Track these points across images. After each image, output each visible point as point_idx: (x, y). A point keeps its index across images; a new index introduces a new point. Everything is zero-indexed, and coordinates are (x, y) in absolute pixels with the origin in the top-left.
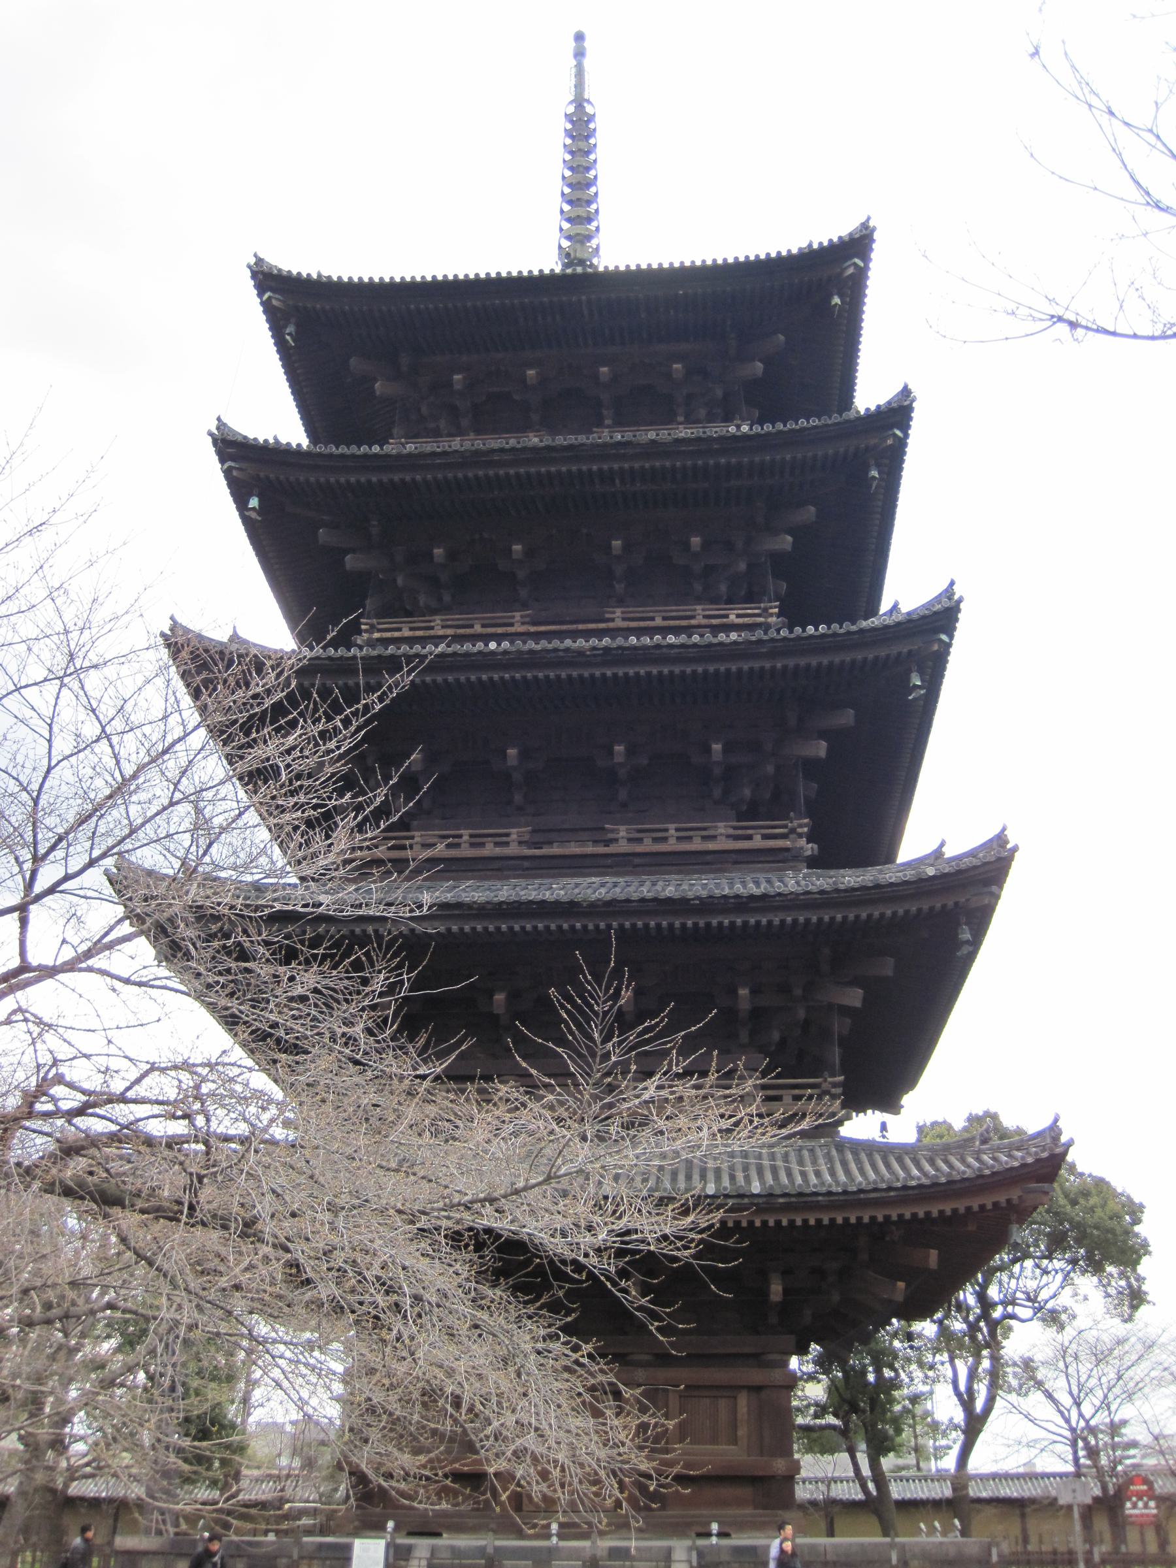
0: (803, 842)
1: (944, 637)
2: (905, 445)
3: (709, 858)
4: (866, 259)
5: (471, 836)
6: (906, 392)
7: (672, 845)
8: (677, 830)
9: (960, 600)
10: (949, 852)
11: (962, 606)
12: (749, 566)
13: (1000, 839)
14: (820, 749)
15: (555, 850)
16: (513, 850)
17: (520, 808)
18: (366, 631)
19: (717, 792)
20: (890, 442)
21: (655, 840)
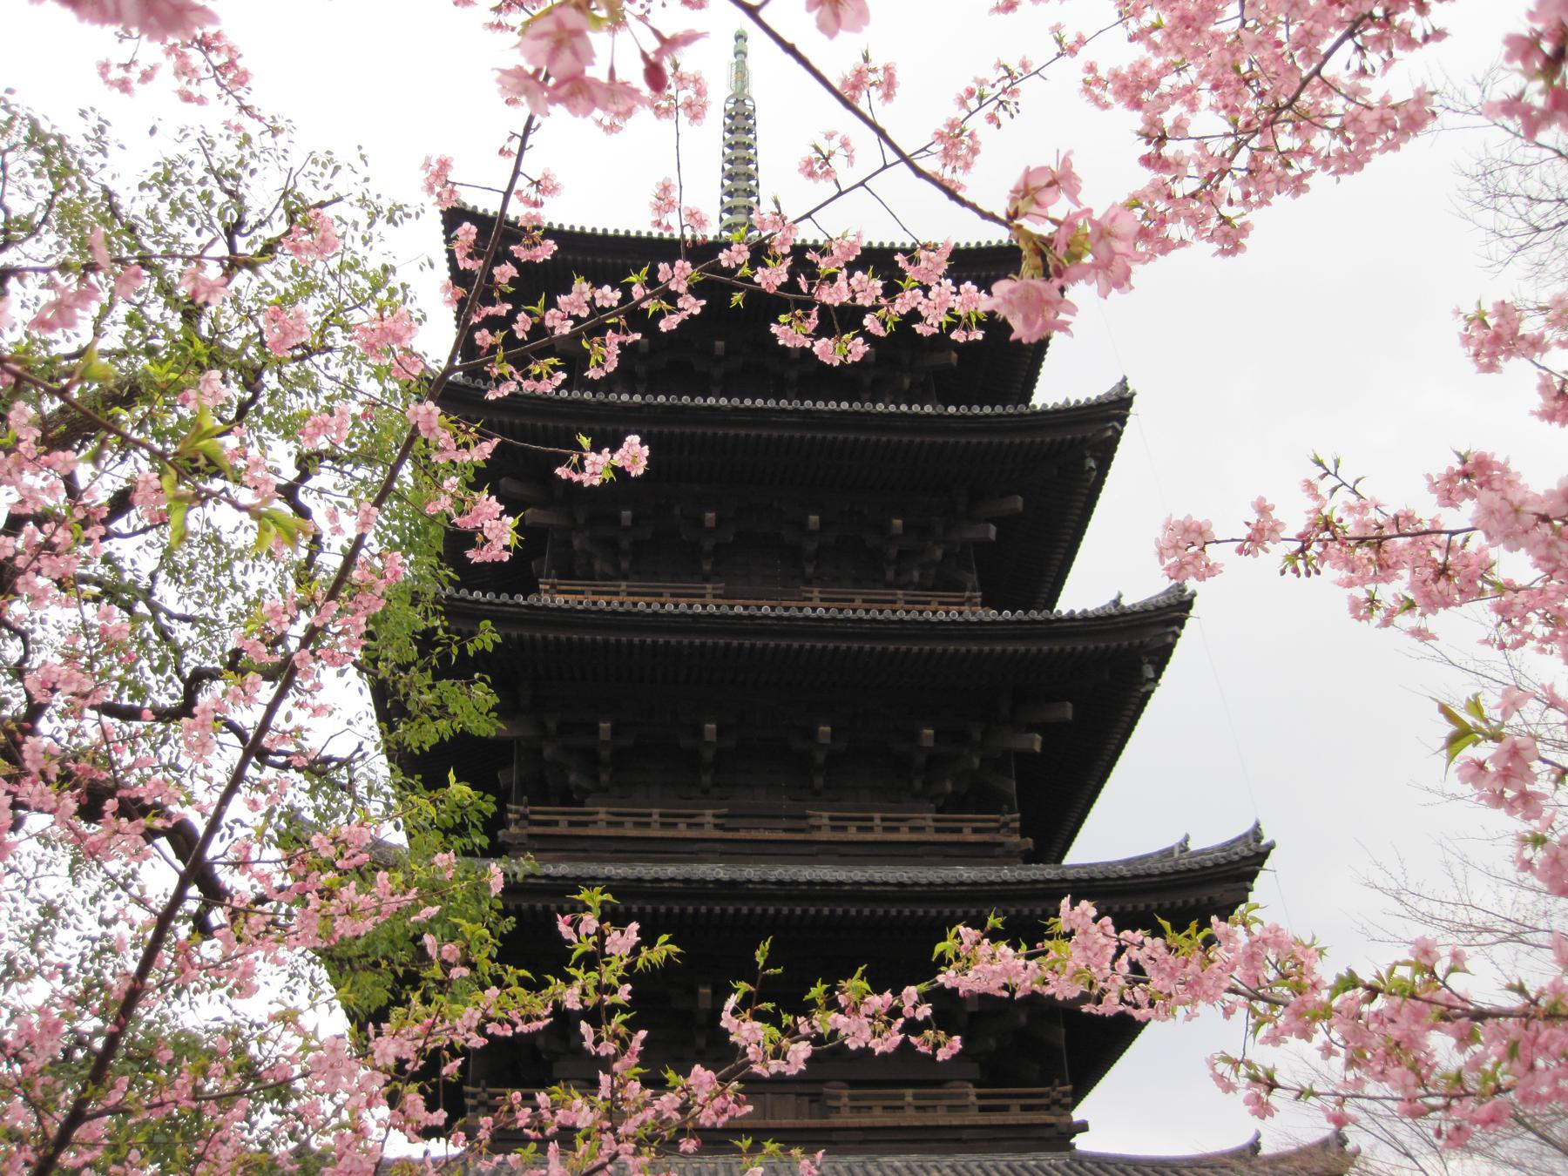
0: (1016, 839)
1: (1176, 628)
2: (1117, 441)
3: (921, 850)
5: (662, 815)
8: (883, 819)
10: (1194, 846)
11: (1196, 600)
12: (945, 555)
13: (1256, 833)
15: (742, 835)
17: (706, 791)
18: (546, 591)
19: (918, 784)
20: (1110, 433)
21: (860, 829)
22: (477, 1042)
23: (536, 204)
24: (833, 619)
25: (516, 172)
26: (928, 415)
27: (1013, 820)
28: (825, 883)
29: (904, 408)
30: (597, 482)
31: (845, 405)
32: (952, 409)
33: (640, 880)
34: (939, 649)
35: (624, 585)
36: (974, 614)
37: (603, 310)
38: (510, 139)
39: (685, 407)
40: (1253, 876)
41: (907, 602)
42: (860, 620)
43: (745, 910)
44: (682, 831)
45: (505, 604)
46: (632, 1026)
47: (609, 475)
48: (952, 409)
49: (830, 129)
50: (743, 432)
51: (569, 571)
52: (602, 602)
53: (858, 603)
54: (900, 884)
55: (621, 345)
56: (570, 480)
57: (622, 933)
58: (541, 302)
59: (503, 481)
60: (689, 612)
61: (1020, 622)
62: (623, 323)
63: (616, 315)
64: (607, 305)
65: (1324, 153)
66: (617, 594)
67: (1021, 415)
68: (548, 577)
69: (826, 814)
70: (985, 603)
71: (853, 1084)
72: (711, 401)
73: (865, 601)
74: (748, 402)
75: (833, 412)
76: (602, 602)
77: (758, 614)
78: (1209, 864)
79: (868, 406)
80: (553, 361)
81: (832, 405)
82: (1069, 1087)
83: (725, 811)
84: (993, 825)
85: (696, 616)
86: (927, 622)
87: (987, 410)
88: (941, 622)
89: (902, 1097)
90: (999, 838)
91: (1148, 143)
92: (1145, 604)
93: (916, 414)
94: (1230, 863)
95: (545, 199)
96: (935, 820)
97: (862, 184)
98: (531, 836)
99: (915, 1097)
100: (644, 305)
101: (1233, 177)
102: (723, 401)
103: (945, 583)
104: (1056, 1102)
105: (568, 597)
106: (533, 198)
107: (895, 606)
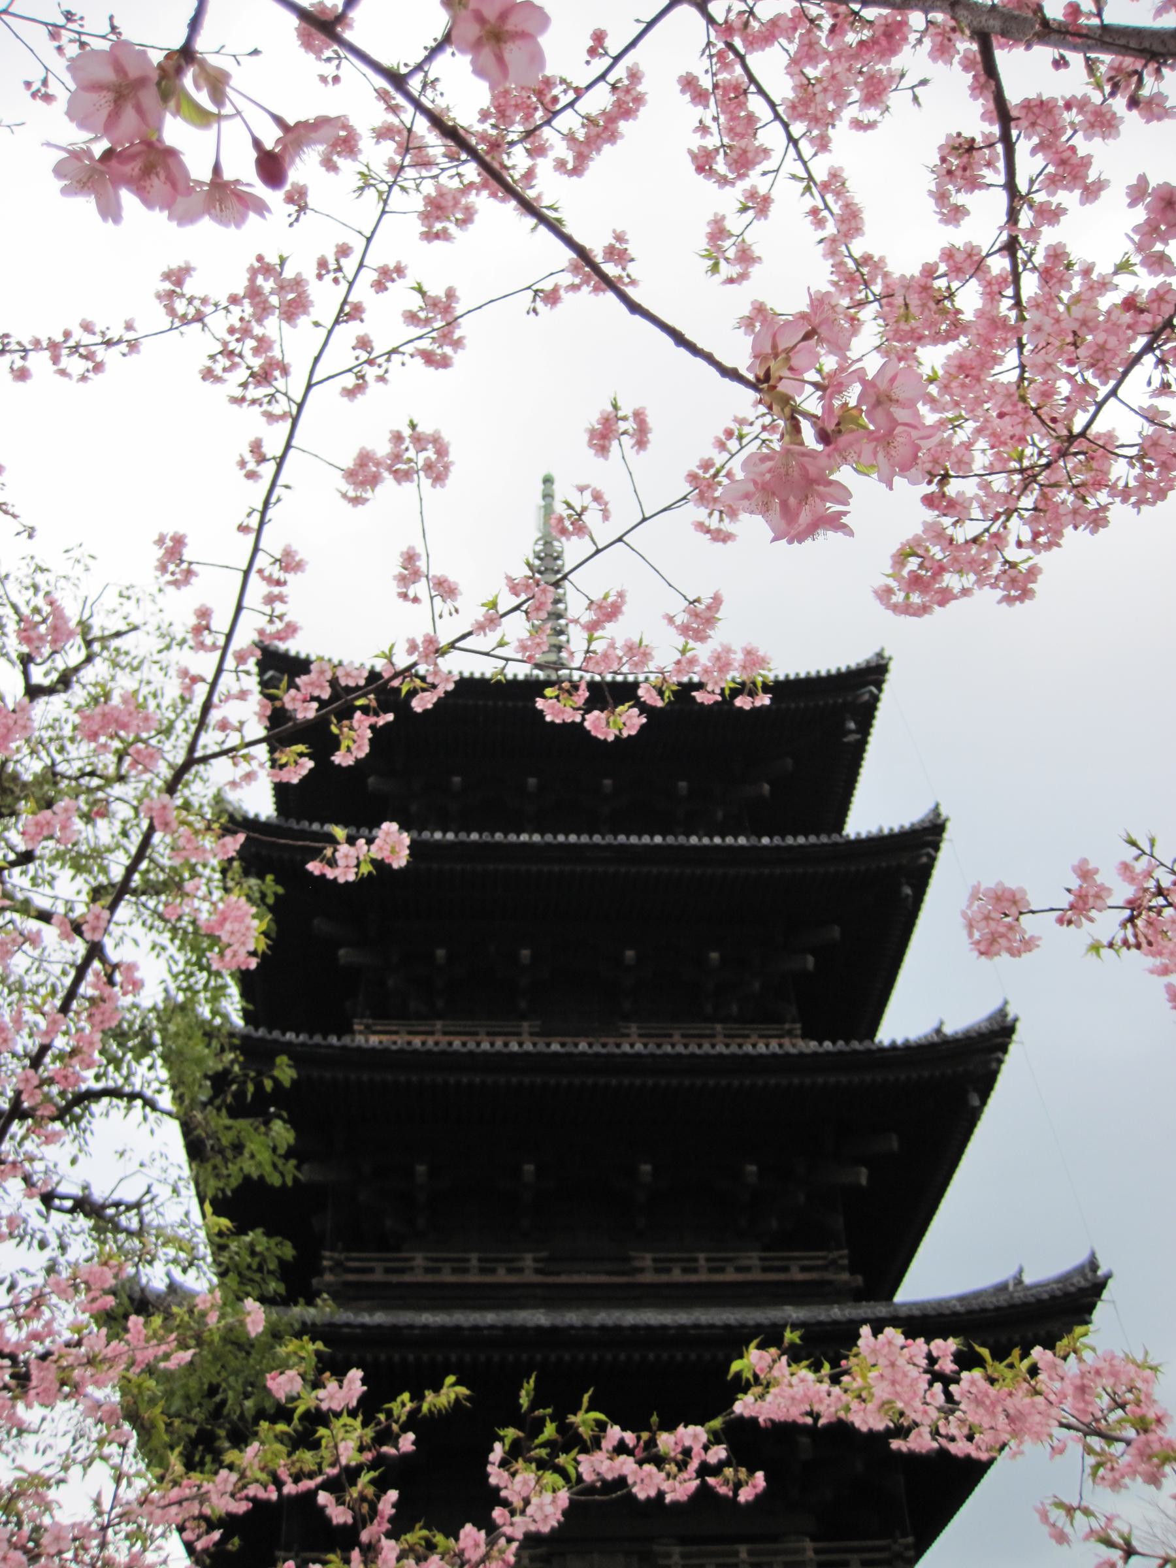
0: (845, 1276)
1: (1000, 1055)
4: (879, 684)
6: (936, 811)
7: (703, 1277)
9: (1016, 1020)
10: (1028, 1279)
11: (1018, 1026)
14: (863, 1176)
15: (564, 1279)
16: (530, 1277)
18: (361, 1032)
20: (924, 860)
21: (685, 1271)
22: (241, 1508)
23: (278, 583)
24: (652, 1055)
25: (256, 549)
26: (742, 847)
27: (841, 1257)
28: (649, 1328)
29: (717, 840)
30: (351, 877)
31: (658, 839)
32: (765, 841)
33: (458, 1328)
34: (760, 1082)
35: (439, 1025)
36: (794, 1046)
37: (348, 690)
38: (249, 515)
39: (498, 845)
40: (1091, 1308)
41: (726, 1036)
42: (679, 1055)
43: (567, 1357)
44: (502, 1276)
45: (318, 1046)
46: (381, 1486)
47: (366, 869)
48: (765, 841)
49: (583, 483)
50: (556, 868)
51: (385, 1012)
52: (417, 1041)
53: (677, 1037)
54: (727, 1327)
55: (372, 727)
56: (323, 876)
57: (341, 1382)
58: (284, 684)
59: (316, 922)
60: (505, 1050)
61: (841, 1053)
62: (374, 704)
63: (365, 695)
64: (352, 684)
65: (1121, 484)
66: (431, 1033)
67: (836, 844)
68: (362, 1017)
69: (649, 1256)
70: (807, 1035)
71: (683, 1541)
72: (524, 837)
73: (683, 1036)
74: (561, 838)
75: (646, 846)
76: (417, 1041)
77: (575, 1051)
78: (1045, 1296)
79: (682, 839)
80: (301, 748)
81: (646, 839)
82: (910, 1540)
83: (544, 1254)
84: (820, 1262)
85: (512, 1055)
86: (747, 1056)
87: (801, 840)
88: (761, 1056)
89: (736, 1554)
90: (829, 1276)
91: (930, 482)
92: (968, 1031)
93: (730, 847)
94: (1067, 1295)
95: (290, 577)
96: (762, 1259)
97: (620, 539)
98: (347, 1284)
99: (750, 1553)
100: (395, 683)
101: (1021, 517)
102: (536, 838)
103: (764, 1017)
104: (899, 1556)
105: (384, 1038)
106: (276, 576)
107: (714, 1041)
